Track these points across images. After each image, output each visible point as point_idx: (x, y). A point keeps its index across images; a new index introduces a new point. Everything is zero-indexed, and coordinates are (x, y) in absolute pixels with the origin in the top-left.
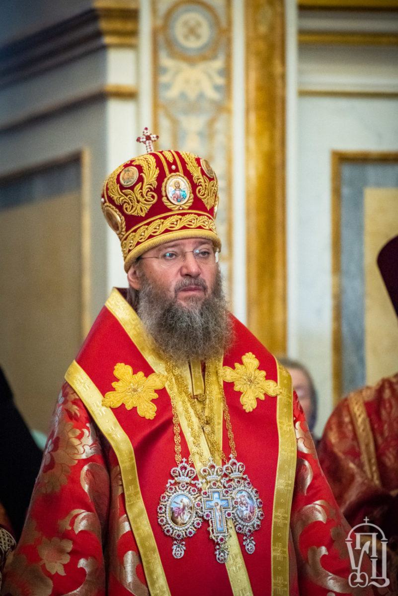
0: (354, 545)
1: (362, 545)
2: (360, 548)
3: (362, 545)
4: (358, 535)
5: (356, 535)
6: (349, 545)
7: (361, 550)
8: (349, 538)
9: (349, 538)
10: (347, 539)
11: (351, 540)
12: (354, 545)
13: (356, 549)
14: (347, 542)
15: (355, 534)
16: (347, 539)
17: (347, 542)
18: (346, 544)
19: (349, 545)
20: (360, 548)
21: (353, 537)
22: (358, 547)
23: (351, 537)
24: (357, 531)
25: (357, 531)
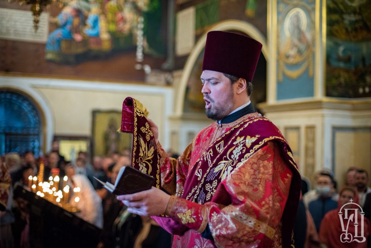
1: (348, 217)
2: (348, 218)
3: (348, 217)
4: (346, 210)
5: (345, 210)
6: (341, 216)
7: (347, 220)
8: (340, 212)
9: (340, 212)
10: (339, 213)
11: (342, 213)
12: (343, 216)
13: (344, 218)
14: (339, 215)
15: (344, 209)
16: (339, 213)
17: (339, 215)
18: (339, 215)
19: (341, 216)
20: (348, 218)
21: (343, 211)
22: (346, 217)
23: (342, 211)
24: (346, 207)
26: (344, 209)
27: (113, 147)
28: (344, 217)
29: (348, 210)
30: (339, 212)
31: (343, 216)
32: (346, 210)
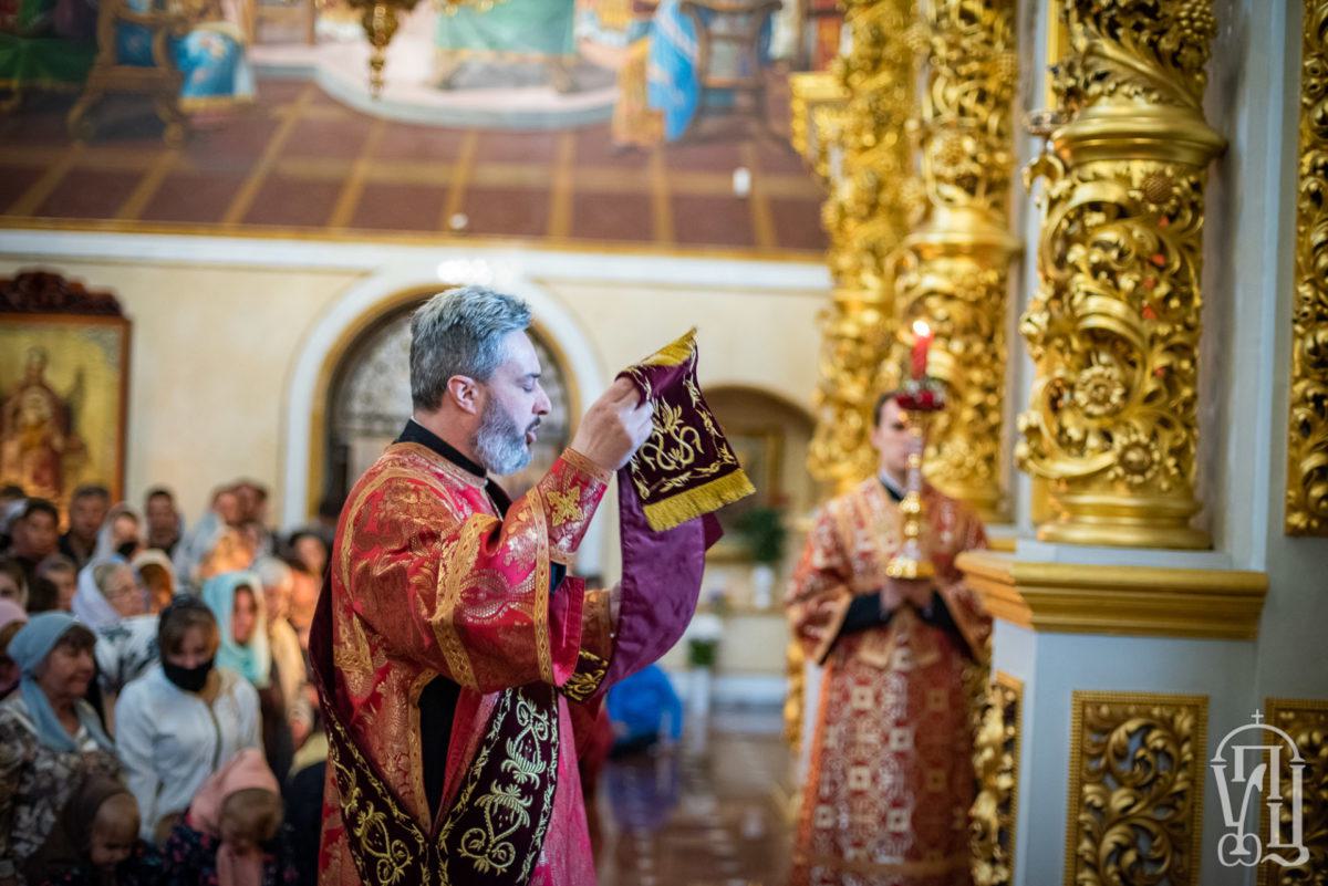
1: (1247, 775)
2: (1243, 780)
3: (1247, 775)
4: (1239, 751)
7: (1245, 784)
8: (1218, 758)
10: (1215, 760)
12: (1229, 773)
13: (1233, 780)
14: (1215, 767)
15: (1233, 747)
16: (1215, 760)
17: (1215, 767)
19: (1219, 771)
20: (1243, 780)
21: (1229, 755)
22: (1239, 777)
23: (1223, 755)
24: (1237, 740)
25: (1237, 740)
26: (1233, 747)
27: (840, 605)
28: (1233, 776)
29: (1245, 750)
30: (1214, 757)
31: (1229, 773)
32: (1239, 751)
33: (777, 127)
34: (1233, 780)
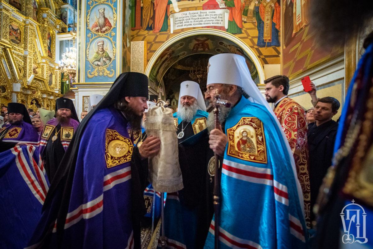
0: (345, 217)
1: (350, 218)
2: (349, 219)
3: (350, 218)
4: (348, 211)
7: (349, 221)
8: (342, 213)
12: (345, 217)
15: (346, 210)
20: (349, 219)
22: (348, 218)
23: (344, 212)
26: (346, 210)
28: (346, 218)
30: (341, 212)
33: (261, 59)
34: (346, 219)
